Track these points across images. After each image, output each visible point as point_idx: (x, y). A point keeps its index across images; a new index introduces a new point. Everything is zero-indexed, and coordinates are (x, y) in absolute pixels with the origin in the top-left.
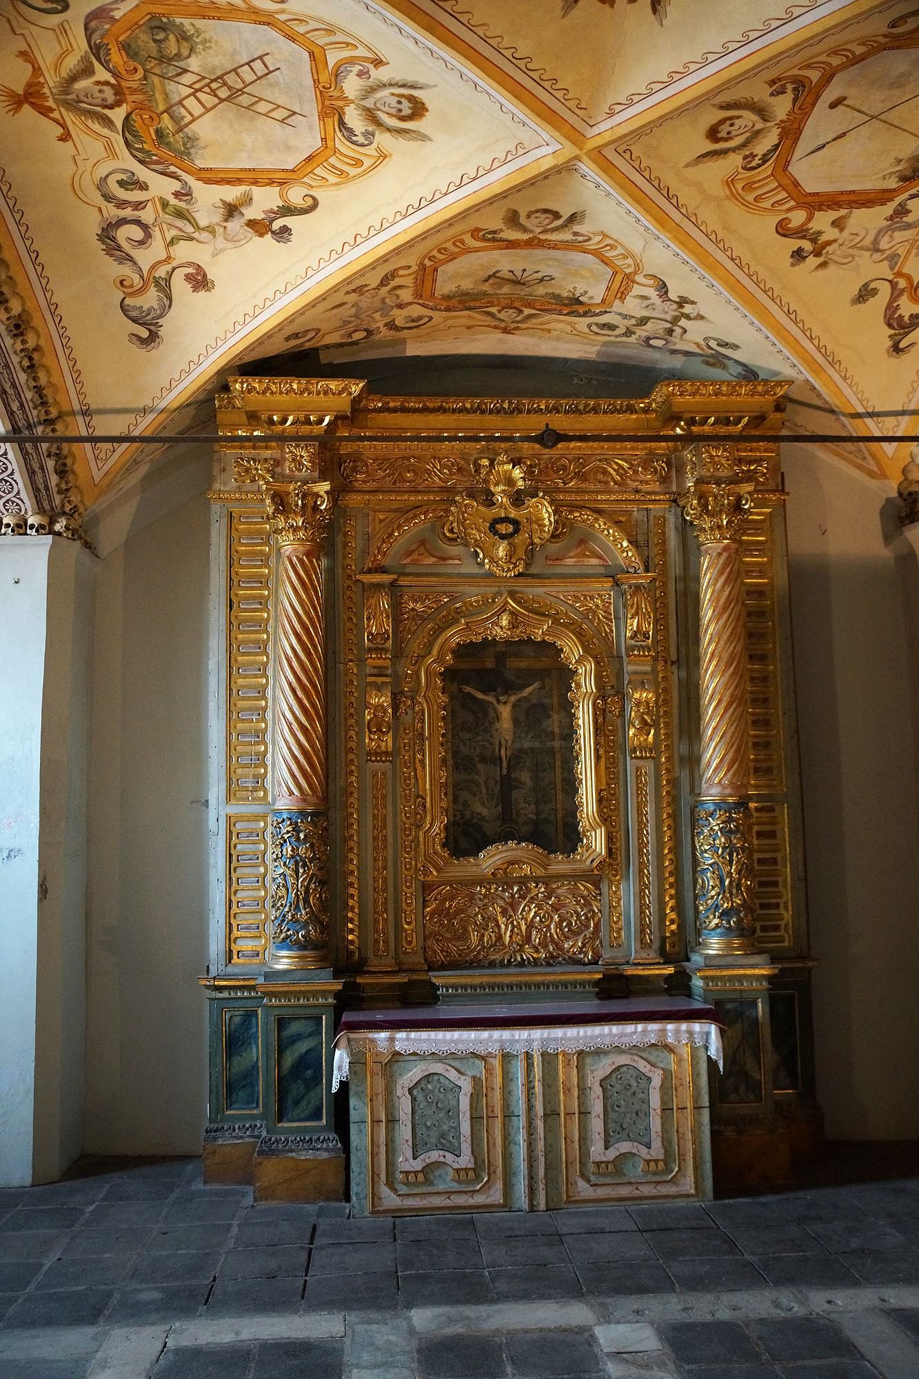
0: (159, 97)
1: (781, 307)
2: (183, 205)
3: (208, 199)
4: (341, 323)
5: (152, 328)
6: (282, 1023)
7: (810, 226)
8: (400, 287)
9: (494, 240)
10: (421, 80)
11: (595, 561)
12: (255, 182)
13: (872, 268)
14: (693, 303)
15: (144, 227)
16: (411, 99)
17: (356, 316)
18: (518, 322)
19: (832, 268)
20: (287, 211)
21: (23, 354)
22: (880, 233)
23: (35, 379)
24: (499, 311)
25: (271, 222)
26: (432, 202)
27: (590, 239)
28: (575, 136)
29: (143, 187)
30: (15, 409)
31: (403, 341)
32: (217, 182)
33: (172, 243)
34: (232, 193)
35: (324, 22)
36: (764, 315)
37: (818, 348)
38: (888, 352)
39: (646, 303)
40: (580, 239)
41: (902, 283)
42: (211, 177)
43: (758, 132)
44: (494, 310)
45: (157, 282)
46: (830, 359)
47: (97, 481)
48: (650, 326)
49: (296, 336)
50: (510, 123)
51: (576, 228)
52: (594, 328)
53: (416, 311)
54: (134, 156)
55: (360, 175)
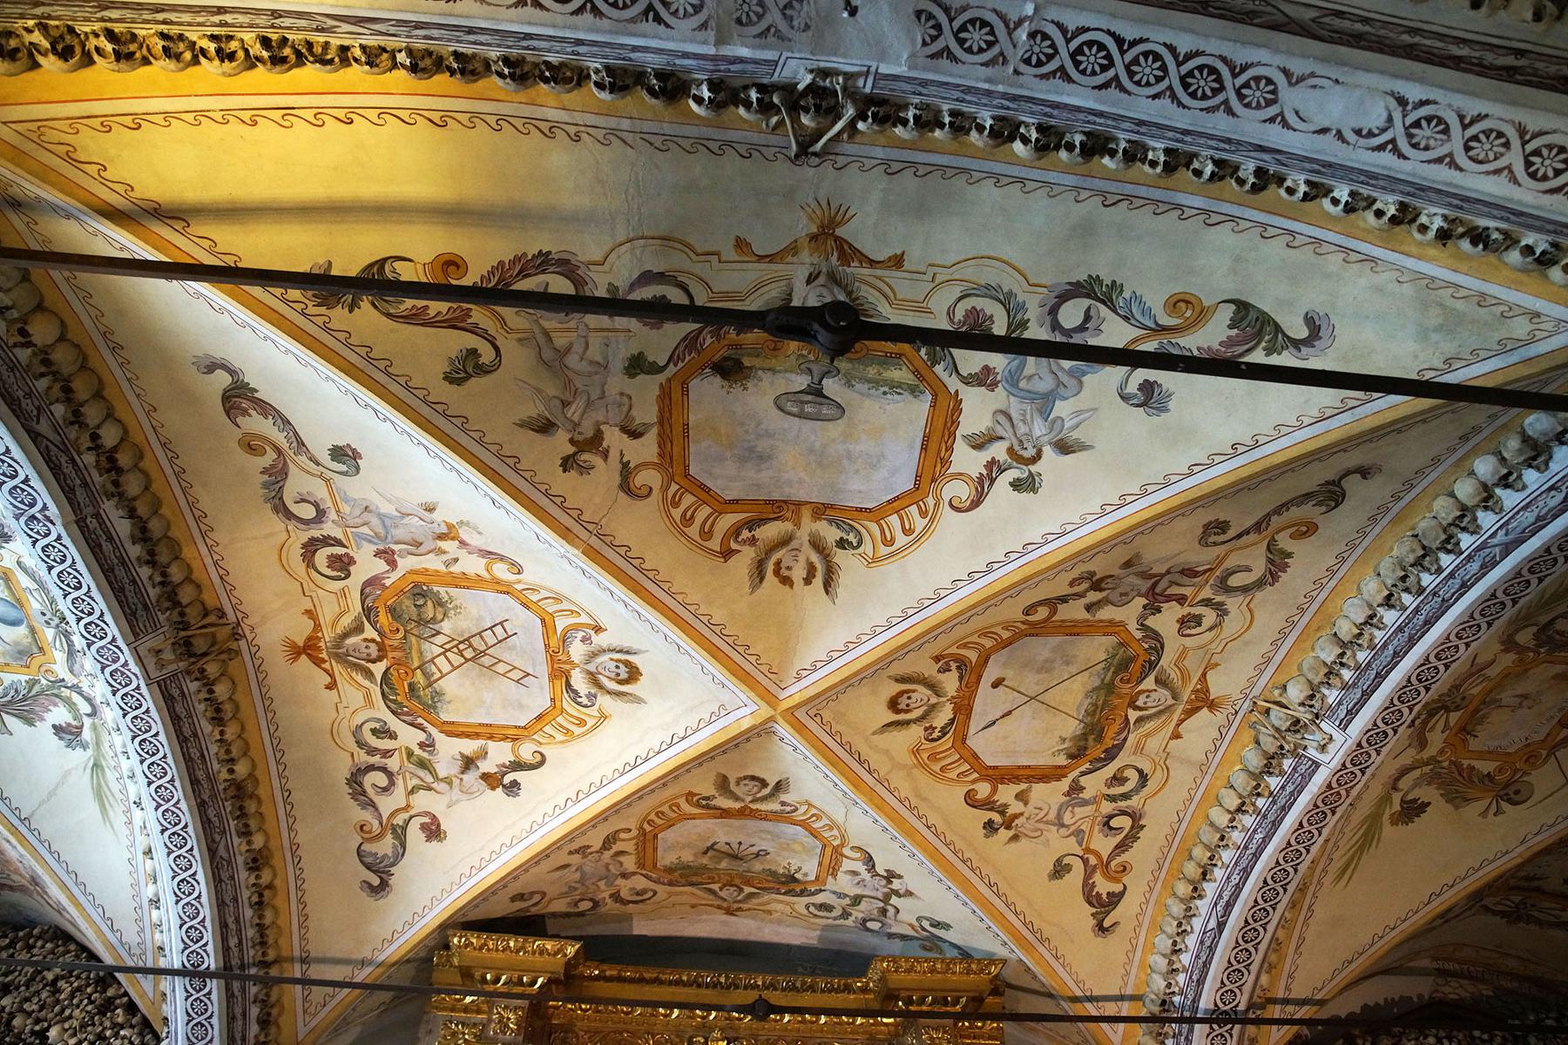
0: (415, 655)
1: (981, 878)
2: (425, 755)
3: (449, 750)
4: (565, 889)
5: (384, 876)
7: (996, 798)
9: (708, 807)
10: (635, 646)
12: (491, 737)
13: (1060, 844)
14: (900, 877)
15: (390, 774)
16: (627, 664)
17: (582, 881)
18: (740, 902)
19: (1024, 842)
20: (518, 766)
21: (254, 889)
22: (1061, 810)
23: (261, 917)
24: (721, 889)
25: (503, 776)
26: (646, 760)
27: (797, 809)
28: (769, 698)
29: (393, 736)
31: (629, 918)
32: (457, 736)
33: (412, 792)
34: (469, 746)
35: (551, 591)
36: (966, 885)
37: (1025, 924)
39: (858, 879)
40: (788, 809)
41: (1093, 861)
42: (453, 730)
43: (934, 706)
44: (715, 887)
46: (1038, 936)
48: (864, 905)
49: (520, 897)
50: (711, 685)
51: (784, 797)
52: (812, 909)
53: (640, 882)
54: (388, 707)
55: (583, 735)
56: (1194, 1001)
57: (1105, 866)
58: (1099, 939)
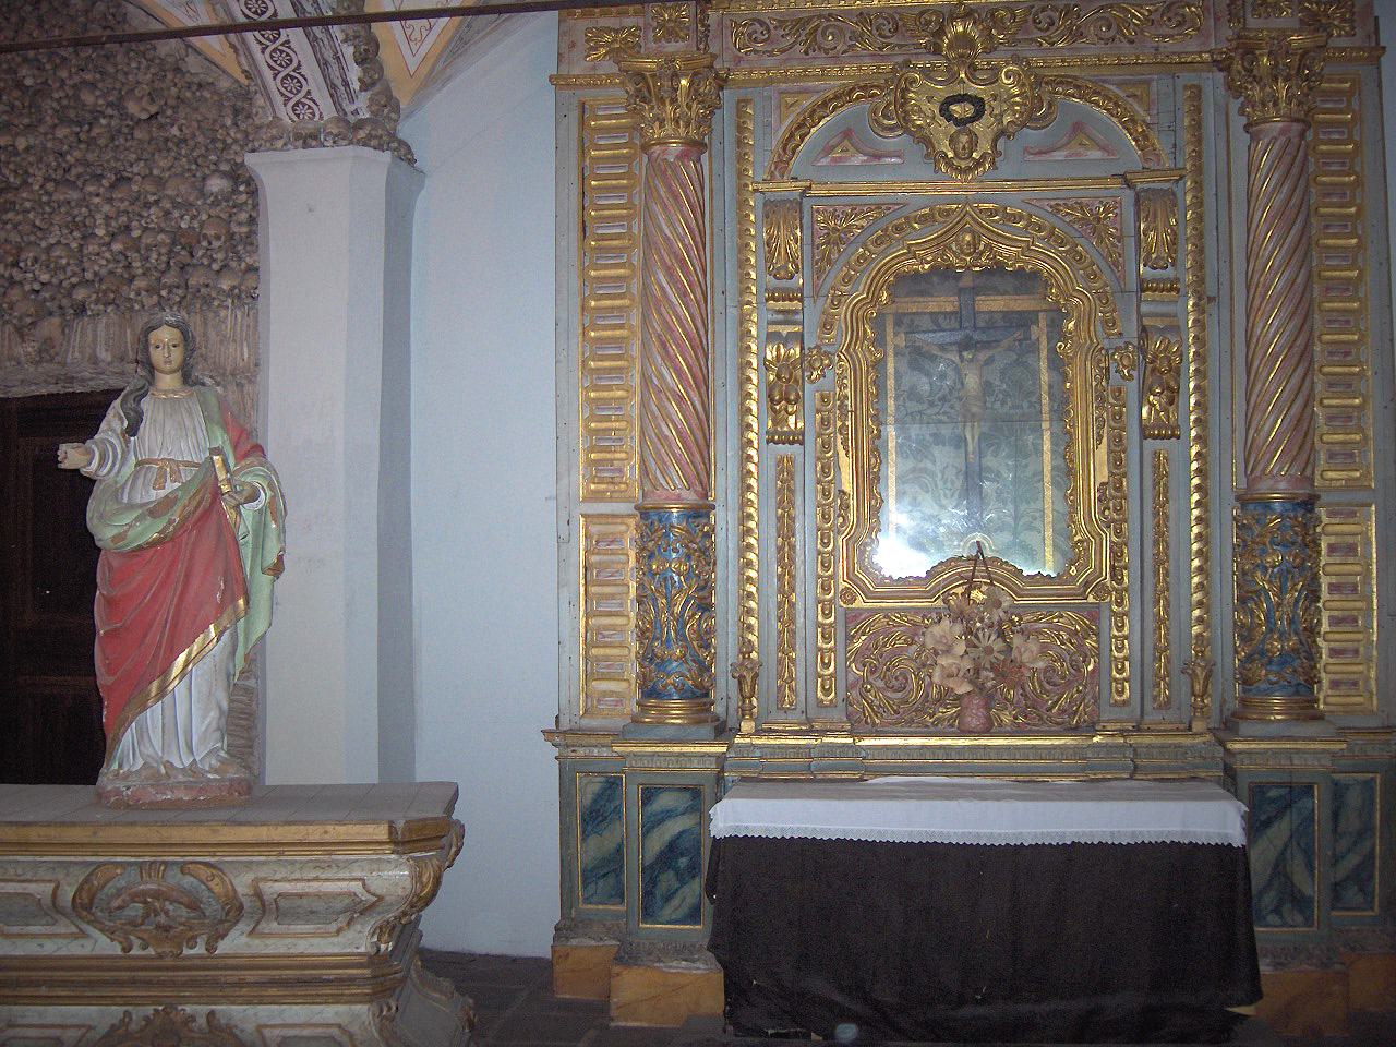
6: (649, 794)
11: (1096, 154)
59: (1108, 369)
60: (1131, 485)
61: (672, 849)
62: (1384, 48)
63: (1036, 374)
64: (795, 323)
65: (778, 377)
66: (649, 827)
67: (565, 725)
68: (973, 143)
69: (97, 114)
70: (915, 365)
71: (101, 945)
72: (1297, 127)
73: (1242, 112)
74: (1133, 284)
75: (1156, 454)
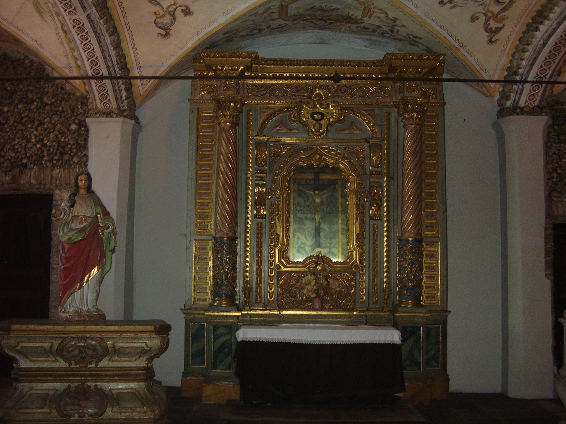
5: (167, 30)
6: (216, 328)
8: (273, 13)
11: (358, 132)
19: (458, 8)
24: (317, 21)
30: (109, 65)
37: (455, 40)
38: (487, 42)
39: (379, 20)
41: (489, 15)
44: (314, 21)
45: (170, 13)
47: (142, 93)
49: (228, 32)
52: (359, 29)
56: (528, 72)
57: (495, 17)
58: (489, 46)
59: (360, 198)
60: (366, 234)
61: (223, 346)
62: (445, 103)
63: (337, 199)
64: (264, 181)
65: (258, 197)
66: (215, 339)
67: (187, 307)
68: (321, 127)
69: (33, 101)
70: (299, 195)
71: (62, 364)
72: (418, 127)
73: (402, 121)
74: (368, 173)
75: (374, 225)
